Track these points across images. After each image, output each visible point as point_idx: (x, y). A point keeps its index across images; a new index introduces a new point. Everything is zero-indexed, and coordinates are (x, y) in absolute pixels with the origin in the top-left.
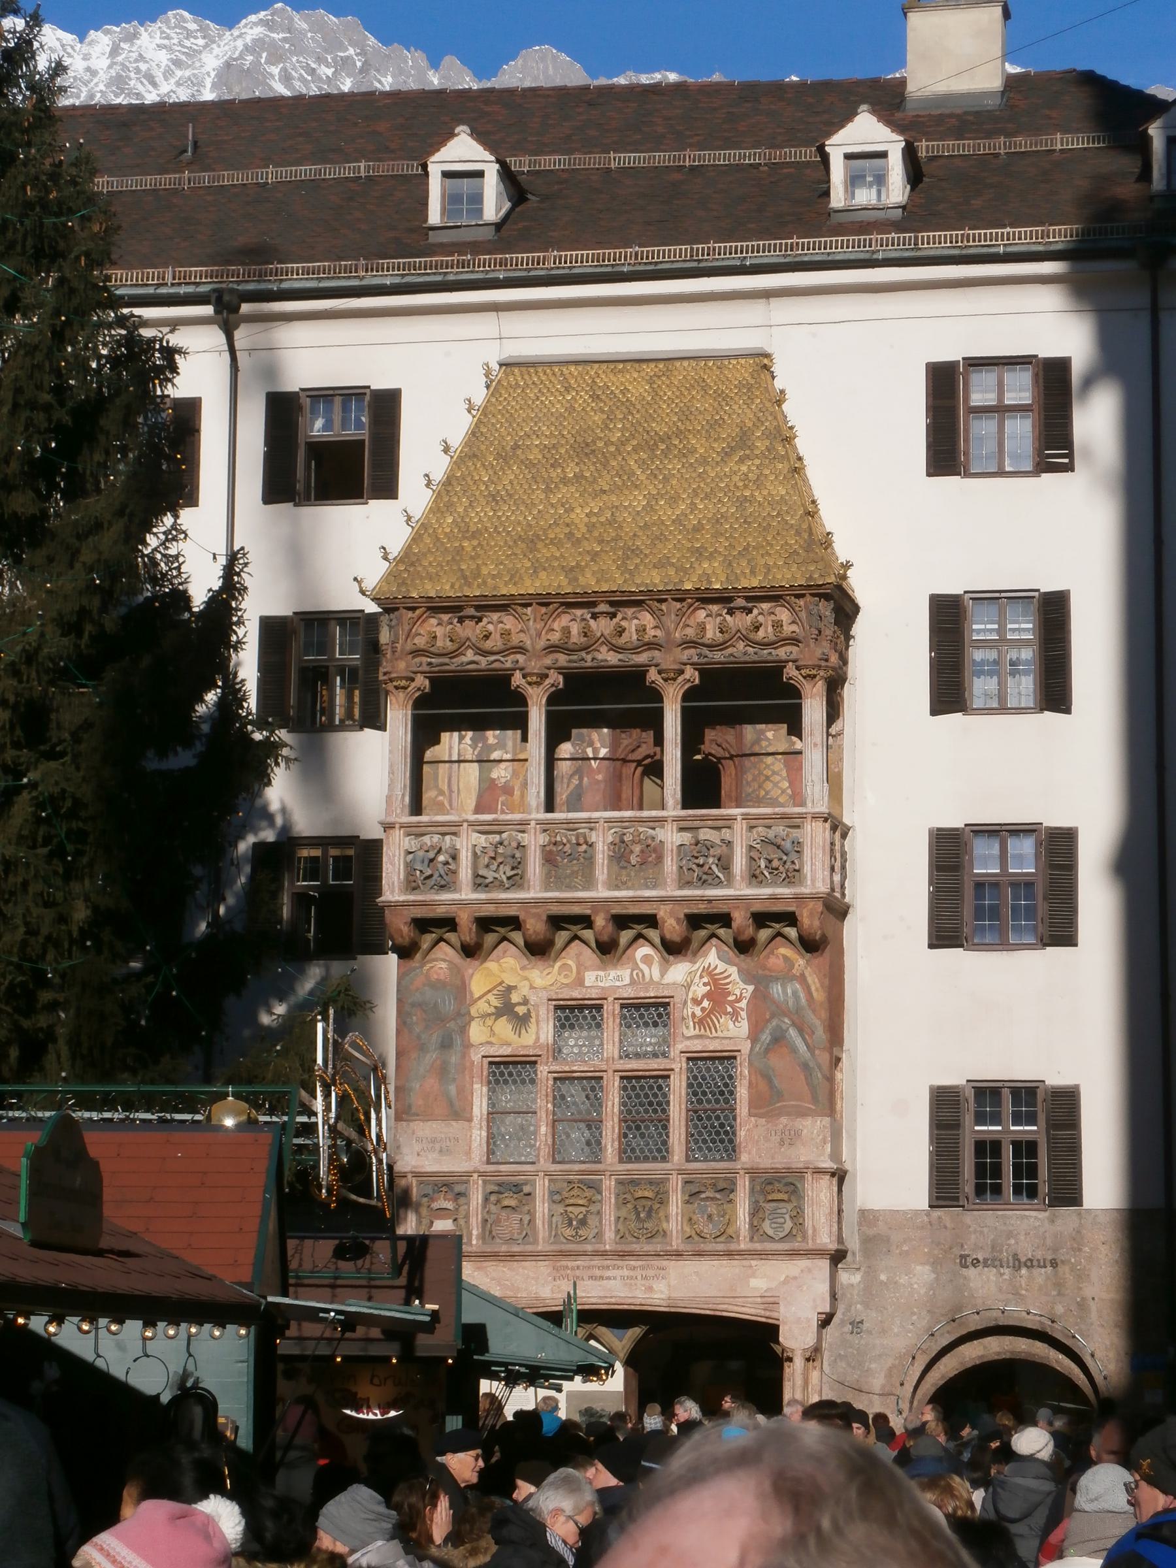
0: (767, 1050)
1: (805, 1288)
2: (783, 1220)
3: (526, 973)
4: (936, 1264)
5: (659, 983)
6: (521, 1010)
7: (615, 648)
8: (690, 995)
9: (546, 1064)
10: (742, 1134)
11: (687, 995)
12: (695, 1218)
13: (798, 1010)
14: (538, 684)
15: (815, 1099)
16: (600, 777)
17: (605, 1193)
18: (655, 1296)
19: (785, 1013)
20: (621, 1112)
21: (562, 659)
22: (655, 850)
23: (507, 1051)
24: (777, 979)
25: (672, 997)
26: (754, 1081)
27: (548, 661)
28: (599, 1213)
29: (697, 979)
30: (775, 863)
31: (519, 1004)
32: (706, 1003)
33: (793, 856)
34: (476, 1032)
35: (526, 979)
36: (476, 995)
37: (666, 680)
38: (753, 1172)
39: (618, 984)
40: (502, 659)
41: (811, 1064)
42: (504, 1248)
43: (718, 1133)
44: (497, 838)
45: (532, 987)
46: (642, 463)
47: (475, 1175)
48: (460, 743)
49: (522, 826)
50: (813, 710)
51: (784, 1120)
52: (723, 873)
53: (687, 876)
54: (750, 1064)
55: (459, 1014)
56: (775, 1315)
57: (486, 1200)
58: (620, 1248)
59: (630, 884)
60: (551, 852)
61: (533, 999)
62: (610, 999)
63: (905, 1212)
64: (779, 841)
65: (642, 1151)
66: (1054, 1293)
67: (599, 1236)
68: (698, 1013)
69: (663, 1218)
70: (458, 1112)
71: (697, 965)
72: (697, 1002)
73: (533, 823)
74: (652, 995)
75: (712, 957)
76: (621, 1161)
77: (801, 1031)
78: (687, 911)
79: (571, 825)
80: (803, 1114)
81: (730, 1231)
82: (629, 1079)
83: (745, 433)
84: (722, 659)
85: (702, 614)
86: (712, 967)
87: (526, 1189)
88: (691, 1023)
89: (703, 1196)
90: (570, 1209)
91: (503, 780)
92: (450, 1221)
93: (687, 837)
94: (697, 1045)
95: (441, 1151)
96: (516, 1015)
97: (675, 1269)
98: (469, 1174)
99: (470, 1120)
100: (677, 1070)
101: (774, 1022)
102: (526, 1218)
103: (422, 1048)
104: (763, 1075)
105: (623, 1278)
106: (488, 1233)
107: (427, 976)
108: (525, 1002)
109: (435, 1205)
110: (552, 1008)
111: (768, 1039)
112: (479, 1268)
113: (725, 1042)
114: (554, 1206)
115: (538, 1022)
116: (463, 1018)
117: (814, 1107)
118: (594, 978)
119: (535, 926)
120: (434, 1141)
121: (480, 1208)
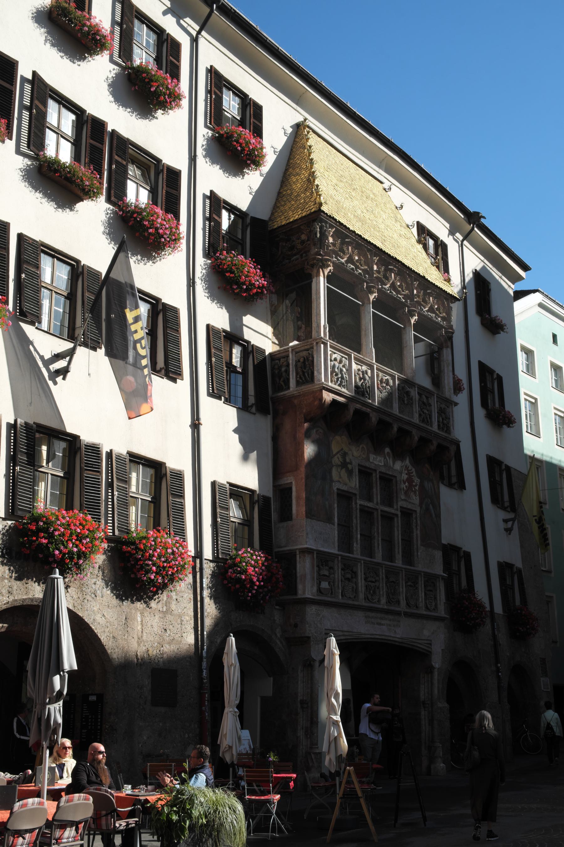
6: (350, 466)
18: (398, 636)
23: (345, 488)
25: (395, 477)
29: (404, 471)
32: (407, 484)
34: (335, 473)
36: (334, 453)
45: (353, 456)
56: (430, 650)
61: (354, 463)
62: (378, 472)
67: (379, 601)
74: (391, 473)
90: (370, 583)
92: (327, 583)
98: (336, 556)
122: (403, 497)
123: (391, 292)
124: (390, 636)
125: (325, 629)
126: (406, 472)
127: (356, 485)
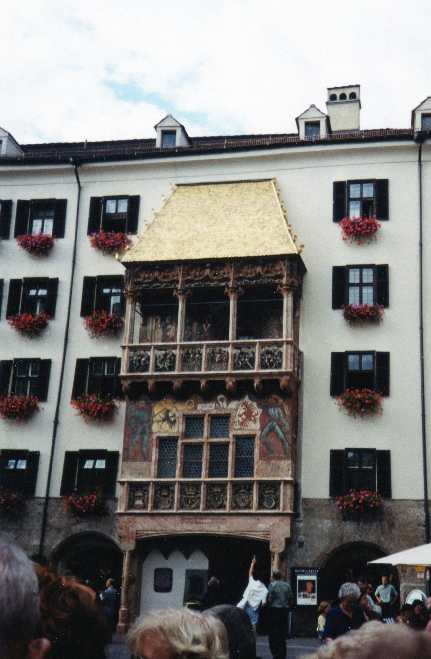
0: (267, 434)
1: (280, 528)
2: (271, 502)
3: (175, 405)
4: (332, 519)
5: (225, 409)
6: (172, 419)
7: (212, 281)
8: (238, 413)
9: (182, 439)
10: (256, 467)
11: (236, 413)
12: (237, 500)
13: (279, 419)
14: (183, 294)
15: (285, 453)
16: (207, 335)
17: (202, 490)
18: (221, 530)
19: (275, 420)
20: (210, 459)
21: (193, 285)
22: (225, 356)
23: (166, 435)
24: (271, 407)
25: (230, 414)
26: (261, 447)
27: (187, 286)
28: (199, 498)
30: (271, 360)
31: (172, 417)
33: (278, 358)
34: (155, 427)
35: (175, 407)
37: (231, 292)
38: (260, 483)
39: (210, 409)
40: (169, 284)
41: (284, 439)
42: (162, 511)
43: (247, 467)
44: (164, 352)
45: (177, 410)
46: (226, 216)
47: (151, 483)
48: (156, 323)
49: (175, 347)
50: (287, 302)
51: (273, 461)
52: (251, 365)
53: (237, 366)
54: (260, 440)
55: (148, 421)
56: (268, 539)
57: (156, 493)
58: (206, 512)
59: (215, 369)
60: (185, 357)
61: (177, 415)
62: (207, 415)
63: (320, 500)
64: (273, 351)
65: (217, 474)
66: (380, 532)
67: (198, 507)
68: (240, 419)
69: (225, 501)
70: (146, 458)
71: (241, 402)
72: (240, 416)
73: (178, 346)
74: (223, 413)
75: (247, 399)
76: (209, 477)
77: (280, 427)
78: (237, 379)
79: (194, 347)
80: (280, 459)
81: (251, 505)
82: (212, 445)
83: (264, 206)
84: (253, 283)
85: (246, 268)
86: (246, 402)
87: (172, 488)
88: (237, 424)
89: (240, 491)
90: (188, 496)
91: (171, 336)
93: (237, 352)
94: (240, 433)
95: (139, 474)
96: (171, 421)
97: (229, 520)
99: (150, 461)
100: (231, 442)
101: (270, 423)
102: (171, 500)
103: (134, 433)
104: (265, 444)
105: (208, 523)
106: (155, 506)
107: (137, 406)
108: (174, 416)
109: (136, 495)
110: (185, 419)
111: (268, 430)
112: (152, 519)
113: (251, 431)
114: (182, 495)
115: (179, 423)
116: (150, 421)
117: (284, 456)
118: (201, 407)
119: (177, 384)
120: (136, 469)
121: (153, 496)
122: (237, 427)
123: (205, 284)
124: (213, 531)
125: (137, 531)
126: (244, 407)
127: (178, 430)
